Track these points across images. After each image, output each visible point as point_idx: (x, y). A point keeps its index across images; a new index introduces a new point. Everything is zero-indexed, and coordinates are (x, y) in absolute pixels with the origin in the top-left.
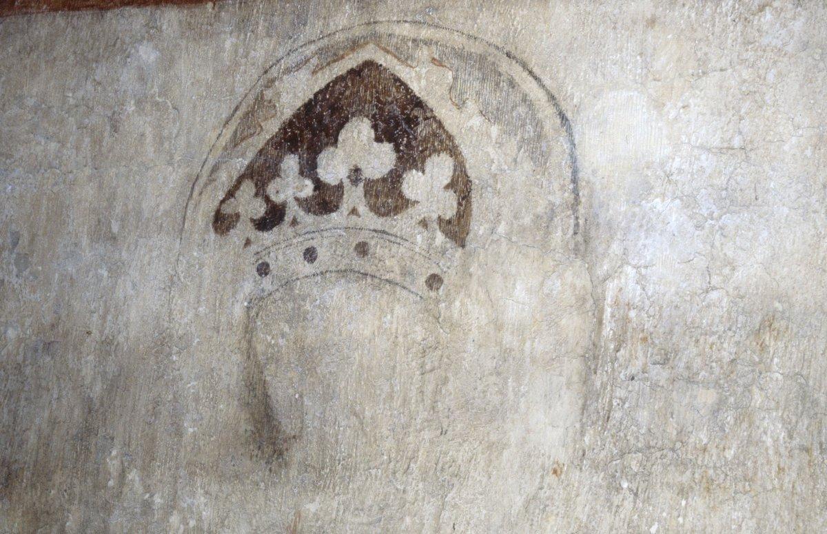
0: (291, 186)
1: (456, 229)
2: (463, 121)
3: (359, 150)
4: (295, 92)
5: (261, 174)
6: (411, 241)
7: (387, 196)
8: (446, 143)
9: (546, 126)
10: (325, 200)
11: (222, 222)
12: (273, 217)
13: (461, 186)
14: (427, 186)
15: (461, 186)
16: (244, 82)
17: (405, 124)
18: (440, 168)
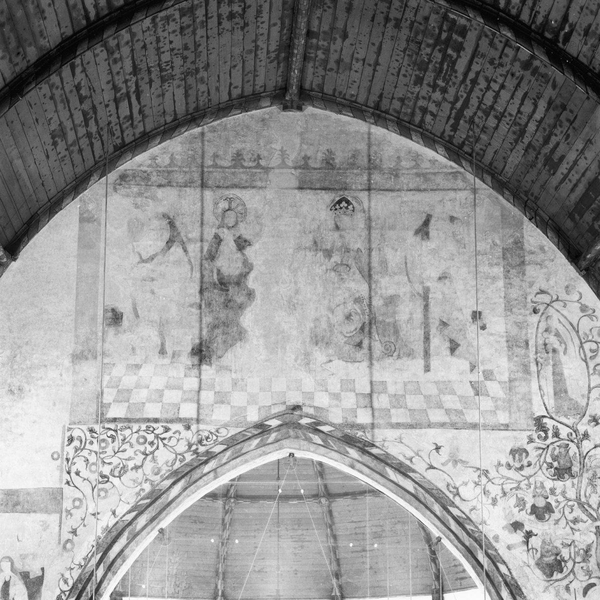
0: (337, 207)
1: (353, 211)
2: (354, 202)
3: (344, 204)
4: (337, 199)
5: (335, 206)
6: (349, 212)
7: (347, 208)
8: (352, 204)
9: (360, 203)
10: (341, 208)
11: (331, 210)
12: (336, 209)
13: (353, 207)
14: (350, 207)
15: (353, 207)
16: (332, 198)
17: (348, 202)
18: (351, 206)
